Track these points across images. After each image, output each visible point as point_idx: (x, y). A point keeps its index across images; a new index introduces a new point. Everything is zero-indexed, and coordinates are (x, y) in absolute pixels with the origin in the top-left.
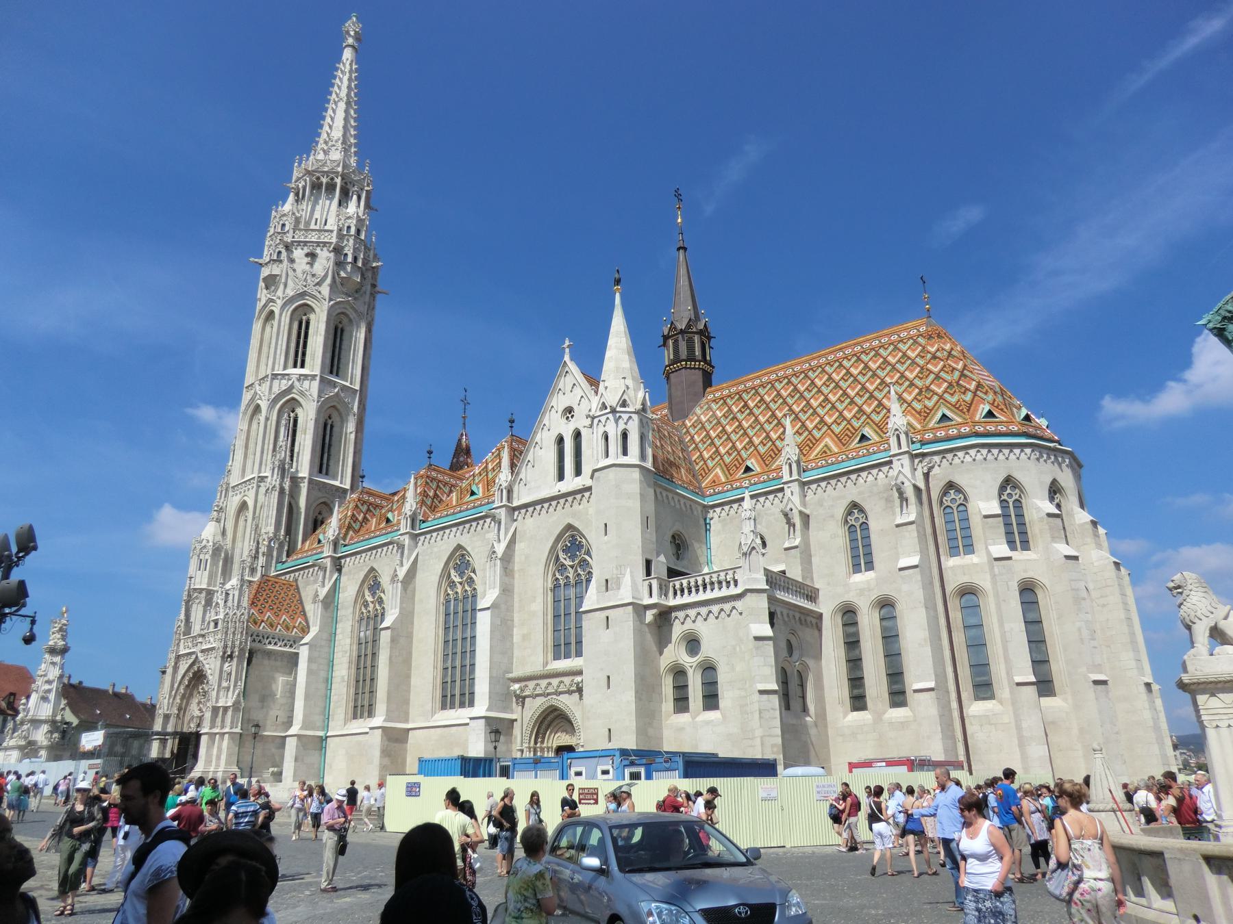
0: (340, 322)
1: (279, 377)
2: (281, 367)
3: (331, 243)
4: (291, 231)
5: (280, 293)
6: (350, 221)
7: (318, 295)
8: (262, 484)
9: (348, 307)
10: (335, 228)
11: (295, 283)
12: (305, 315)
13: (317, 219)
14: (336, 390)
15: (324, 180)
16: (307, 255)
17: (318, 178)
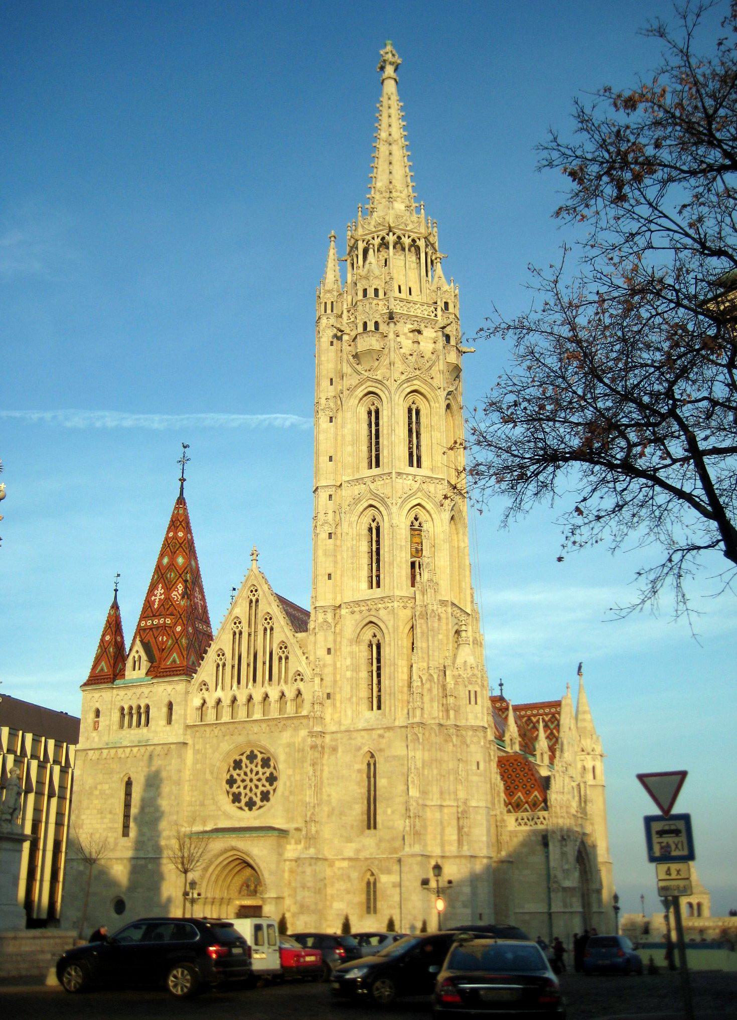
16: (413, 331)
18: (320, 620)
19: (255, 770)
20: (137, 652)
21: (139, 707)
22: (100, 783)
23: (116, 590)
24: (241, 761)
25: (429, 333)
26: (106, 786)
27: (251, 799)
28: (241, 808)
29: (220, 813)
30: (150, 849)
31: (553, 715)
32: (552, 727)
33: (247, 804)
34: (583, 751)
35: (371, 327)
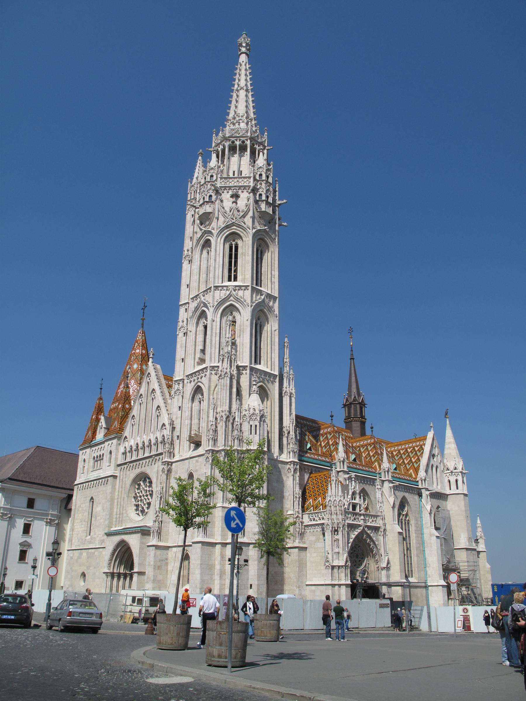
0: (260, 246)
1: (220, 288)
2: (220, 280)
3: (249, 186)
4: (219, 179)
5: (214, 224)
6: (261, 170)
7: (245, 226)
8: (213, 372)
9: (265, 234)
10: (252, 175)
11: (224, 217)
12: (234, 241)
13: (234, 172)
14: (263, 297)
15: (238, 143)
16: (232, 196)
17: (233, 142)
18: (176, 389)
19: (145, 489)
20: (101, 423)
21: (100, 455)
22: (82, 504)
23: (101, 389)
24: (140, 484)
25: (244, 196)
26: (84, 505)
27: (143, 508)
28: (138, 514)
29: (128, 518)
30: (97, 542)
31: (421, 446)
32: (419, 454)
33: (141, 511)
34: (448, 470)
35: (207, 199)
